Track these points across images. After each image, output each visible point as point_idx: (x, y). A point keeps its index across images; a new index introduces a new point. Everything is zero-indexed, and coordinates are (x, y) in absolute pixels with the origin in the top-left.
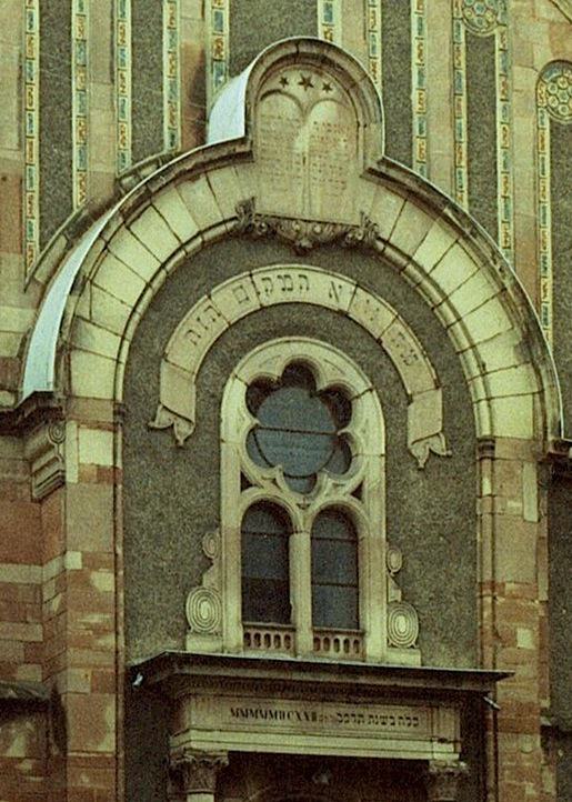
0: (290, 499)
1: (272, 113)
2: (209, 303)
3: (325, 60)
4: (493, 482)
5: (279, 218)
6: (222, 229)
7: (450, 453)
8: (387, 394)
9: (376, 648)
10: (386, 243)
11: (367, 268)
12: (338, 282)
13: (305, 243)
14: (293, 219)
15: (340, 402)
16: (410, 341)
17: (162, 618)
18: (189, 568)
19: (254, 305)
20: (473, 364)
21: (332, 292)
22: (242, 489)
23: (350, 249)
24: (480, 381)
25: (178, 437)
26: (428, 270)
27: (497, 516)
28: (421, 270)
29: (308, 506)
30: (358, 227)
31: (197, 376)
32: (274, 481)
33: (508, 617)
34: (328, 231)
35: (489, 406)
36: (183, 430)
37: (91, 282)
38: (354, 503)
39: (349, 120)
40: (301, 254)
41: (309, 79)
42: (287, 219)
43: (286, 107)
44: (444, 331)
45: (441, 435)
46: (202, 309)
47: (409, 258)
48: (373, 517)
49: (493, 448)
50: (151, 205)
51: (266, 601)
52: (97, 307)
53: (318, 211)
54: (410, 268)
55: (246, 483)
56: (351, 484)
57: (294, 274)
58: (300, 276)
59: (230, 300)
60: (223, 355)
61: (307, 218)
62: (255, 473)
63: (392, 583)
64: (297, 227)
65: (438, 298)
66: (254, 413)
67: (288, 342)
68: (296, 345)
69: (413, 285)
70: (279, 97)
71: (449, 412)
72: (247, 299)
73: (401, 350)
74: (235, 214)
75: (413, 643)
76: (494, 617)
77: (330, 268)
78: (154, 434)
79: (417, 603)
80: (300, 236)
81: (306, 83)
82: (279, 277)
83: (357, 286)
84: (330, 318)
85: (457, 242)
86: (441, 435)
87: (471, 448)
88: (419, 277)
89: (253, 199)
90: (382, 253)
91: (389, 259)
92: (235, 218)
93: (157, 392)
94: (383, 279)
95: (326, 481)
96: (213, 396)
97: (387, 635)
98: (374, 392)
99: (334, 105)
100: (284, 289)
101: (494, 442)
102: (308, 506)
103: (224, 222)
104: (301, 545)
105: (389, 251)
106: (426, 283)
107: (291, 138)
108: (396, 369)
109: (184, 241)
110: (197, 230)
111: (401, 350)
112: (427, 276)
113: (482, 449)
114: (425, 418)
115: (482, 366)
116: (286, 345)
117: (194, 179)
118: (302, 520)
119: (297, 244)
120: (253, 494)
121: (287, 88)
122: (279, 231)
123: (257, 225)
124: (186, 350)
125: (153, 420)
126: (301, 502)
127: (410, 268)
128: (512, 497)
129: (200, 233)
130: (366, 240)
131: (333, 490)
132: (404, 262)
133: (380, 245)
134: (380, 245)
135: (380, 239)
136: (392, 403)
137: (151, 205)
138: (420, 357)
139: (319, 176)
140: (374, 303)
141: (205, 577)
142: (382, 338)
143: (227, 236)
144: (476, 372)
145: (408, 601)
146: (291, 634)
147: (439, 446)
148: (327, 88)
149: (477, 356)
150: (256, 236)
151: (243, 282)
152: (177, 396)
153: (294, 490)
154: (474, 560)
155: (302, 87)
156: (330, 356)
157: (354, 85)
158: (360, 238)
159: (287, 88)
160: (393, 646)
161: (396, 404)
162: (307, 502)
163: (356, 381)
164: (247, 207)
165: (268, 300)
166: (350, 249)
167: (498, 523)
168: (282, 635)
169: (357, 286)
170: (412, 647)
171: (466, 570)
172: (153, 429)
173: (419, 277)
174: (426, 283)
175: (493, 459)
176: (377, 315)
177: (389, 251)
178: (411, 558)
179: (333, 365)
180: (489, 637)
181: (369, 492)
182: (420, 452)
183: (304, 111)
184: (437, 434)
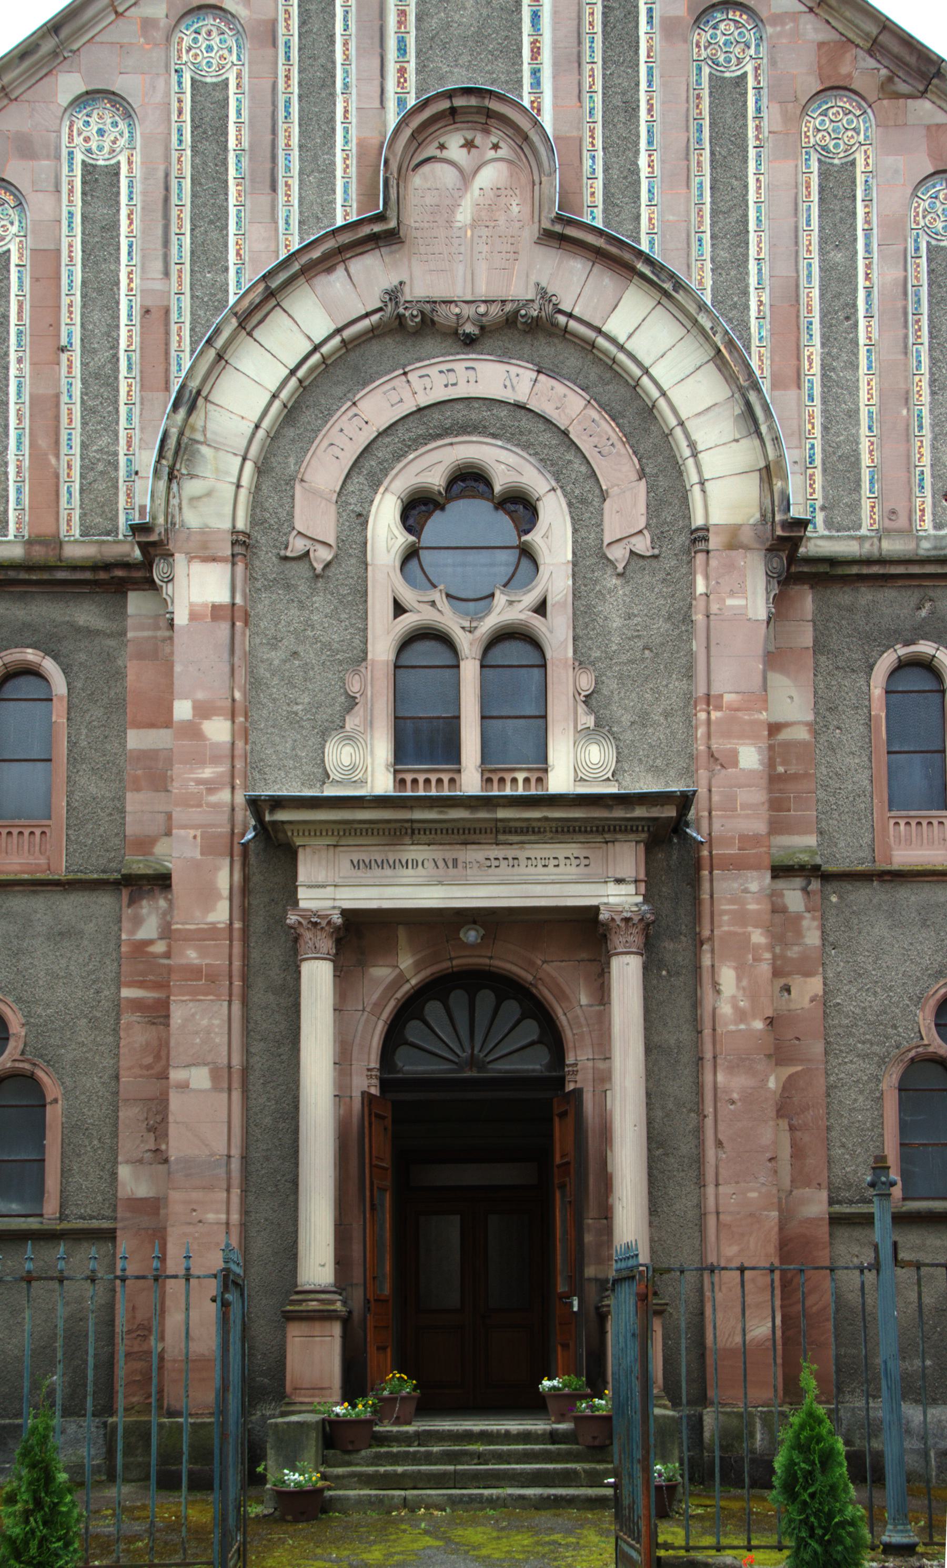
0: (449, 620)
1: (428, 185)
2: (354, 410)
3: (490, 114)
4: (707, 577)
5: (435, 302)
6: (366, 323)
7: (656, 552)
8: (577, 492)
9: (560, 781)
10: (570, 315)
11: (547, 350)
12: (514, 370)
13: (469, 328)
14: (451, 302)
15: (520, 507)
16: (607, 428)
17: (295, 768)
18: (329, 711)
19: (409, 406)
20: (683, 443)
21: (508, 383)
22: (396, 616)
23: (528, 329)
24: (690, 462)
25: (315, 565)
26: (621, 340)
27: (712, 617)
28: (613, 340)
29: (476, 628)
30: (533, 301)
31: (339, 494)
32: (433, 603)
33: (728, 735)
34: (494, 310)
35: (703, 491)
36: (322, 555)
37: (206, 399)
38: (536, 621)
39: (524, 179)
40: (469, 342)
41: (472, 141)
42: (444, 302)
43: (443, 175)
44: (649, 412)
45: (645, 532)
46: (345, 418)
47: (599, 331)
48: (557, 634)
49: (706, 539)
50: (278, 305)
51: (424, 739)
52: (211, 426)
53: (482, 291)
54: (601, 341)
55: (399, 609)
56: (531, 598)
57: (459, 367)
58: (467, 368)
59: (380, 405)
60: (369, 467)
61: (469, 298)
62: (408, 596)
63: (582, 708)
64: (457, 310)
65: (637, 372)
66: (409, 529)
67: (451, 444)
68: (462, 447)
69: (610, 363)
70: (438, 167)
71: (655, 507)
72: (401, 401)
73: (595, 440)
74: (379, 305)
75: (610, 775)
76: (709, 736)
77: (504, 356)
78: (288, 565)
79: (615, 729)
80: (461, 322)
81: (469, 145)
82: (441, 372)
83: (539, 372)
84: (503, 413)
85: (659, 303)
86: (645, 532)
87: (682, 539)
88: (612, 349)
89: (401, 283)
90: (565, 330)
91: (575, 335)
92: (380, 310)
93: (291, 515)
94: (572, 360)
95: (500, 599)
96: (360, 515)
97: (574, 763)
98: (559, 491)
99: (502, 166)
100: (446, 386)
101: (708, 530)
102: (476, 628)
103: (367, 315)
104: (470, 671)
105: (573, 324)
106: (621, 357)
107: (453, 208)
108: (588, 463)
109: (317, 342)
110: (333, 327)
111: (595, 440)
112: (621, 348)
113: (694, 541)
114: (626, 513)
115: (692, 445)
116: (449, 448)
117: (330, 270)
118: (469, 646)
119: (461, 332)
120: (408, 621)
121: (445, 154)
122: (436, 319)
123: (407, 314)
124: (324, 468)
125: (286, 548)
126: (467, 624)
127: (601, 341)
128: (732, 593)
129: (338, 331)
130: (543, 314)
131: (507, 610)
132: (590, 334)
133: (562, 319)
134: (562, 319)
135: (560, 312)
136: (583, 501)
137: (278, 305)
138: (619, 445)
139: (485, 248)
140: (560, 389)
141: (347, 718)
142: (570, 429)
143: (373, 333)
144: (687, 452)
145: (603, 728)
146: (455, 776)
147: (642, 545)
148: (496, 147)
149: (687, 435)
150: (408, 328)
151: (396, 383)
152: (315, 519)
153: (455, 610)
154: (689, 673)
155: (465, 150)
156: (504, 455)
157: (526, 138)
158: (535, 314)
159: (445, 154)
160: (582, 780)
161: (586, 504)
162: (474, 624)
163: (535, 481)
164: (393, 295)
165: (424, 401)
166: (528, 329)
167: (712, 623)
168: (446, 778)
169: (539, 372)
170: (608, 779)
171: (677, 685)
172: (286, 558)
173: (612, 349)
174: (621, 357)
175: (708, 552)
176: (563, 402)
177: (573, 324)
178: (608, 678)
179: (507, 466)
180: (703, 759)
181: (553, 606)
182: (618, 554)
183: (466, 177)
184: (641, 532)
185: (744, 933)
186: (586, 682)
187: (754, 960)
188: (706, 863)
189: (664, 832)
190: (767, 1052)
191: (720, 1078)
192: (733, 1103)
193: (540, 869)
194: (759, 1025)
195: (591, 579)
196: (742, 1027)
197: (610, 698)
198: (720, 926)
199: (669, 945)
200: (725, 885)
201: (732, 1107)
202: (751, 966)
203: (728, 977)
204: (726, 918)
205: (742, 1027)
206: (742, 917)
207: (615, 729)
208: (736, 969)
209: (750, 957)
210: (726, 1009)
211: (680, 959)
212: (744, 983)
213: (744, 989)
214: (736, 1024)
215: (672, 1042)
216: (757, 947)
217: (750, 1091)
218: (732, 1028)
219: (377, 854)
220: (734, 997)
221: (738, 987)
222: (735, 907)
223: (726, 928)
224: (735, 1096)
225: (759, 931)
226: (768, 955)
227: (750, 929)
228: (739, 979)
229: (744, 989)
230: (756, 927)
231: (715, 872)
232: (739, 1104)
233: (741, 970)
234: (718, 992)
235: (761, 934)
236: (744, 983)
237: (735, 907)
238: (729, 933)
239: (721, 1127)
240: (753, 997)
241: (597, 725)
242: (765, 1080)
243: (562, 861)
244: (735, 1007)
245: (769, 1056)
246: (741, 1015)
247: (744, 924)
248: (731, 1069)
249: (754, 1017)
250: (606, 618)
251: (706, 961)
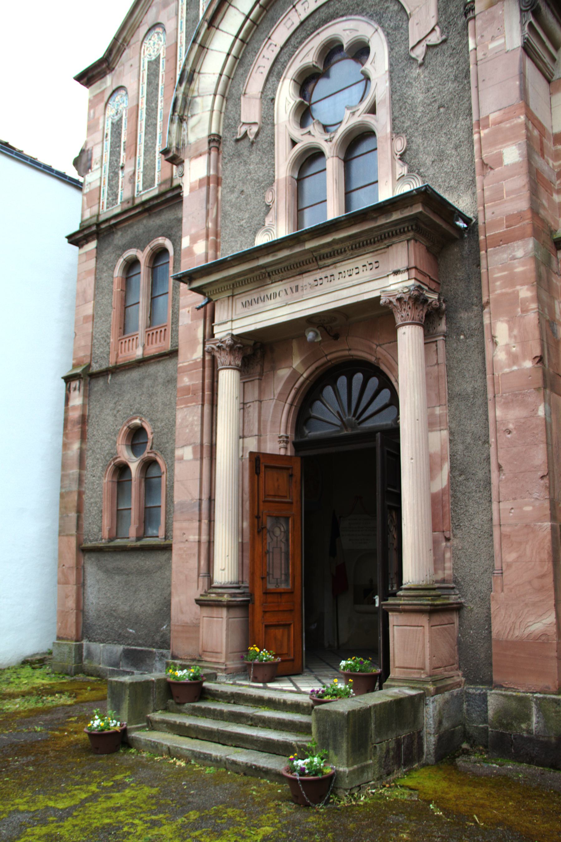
185: (514, 292)
186: (400, 145)
187: (523, 311)
188: (482, 245)
189: (436, 228)
190: (536, 386)
191: (498, 413)
192: (510, 432)
193: (348, 278)
194: (528, 364)
195: (402, 77)
196: (515, 368)
197: (417, 150)
198: (494, 291)
199: (464, 315)
200: (497, 258)
201: (509, 436)
202: (521, 317)
203: (502, 331)
204: (498, 283)
205: (515, 368)
206: (511, 280)
207: (422, 170)
208: (508, 322)
209: (519, 310)
210: (501, 356)
211: (473, 324)
212: (515, 332)
213: (515, 337)
214: (510, 366)
215: (469, 390)
216: (525, 300)
217: (522, 421)
218: (507, 370)
219: (255, 295)
220: (507, 345)
221: (510, 336)
222: (506, 273)
223: (498, 292)
224: (511, 426)
225: (525, 287)
226: (534, 306)
227: (518, 287)
228: (511, 330)
229: (515, 337)
230: (522, 285)
231: (489, 250)
232: (514, 432)
233: (512, 322)
234: (495, 344)
235: (528, 290)
236: (515, 332)
237: (506, 273)
238: (502, 294)
239: (500, 454)
240: (523, 342)
241: (410, 171)
242: (535, 410)
243: (361, 268)
244: (509, 353)
245: (538, 389)
246: (514, 359)
247: (513, 285)
248: (507, 405)
249: (524, 359)
250: (413, 98)
251: (486, 321)
